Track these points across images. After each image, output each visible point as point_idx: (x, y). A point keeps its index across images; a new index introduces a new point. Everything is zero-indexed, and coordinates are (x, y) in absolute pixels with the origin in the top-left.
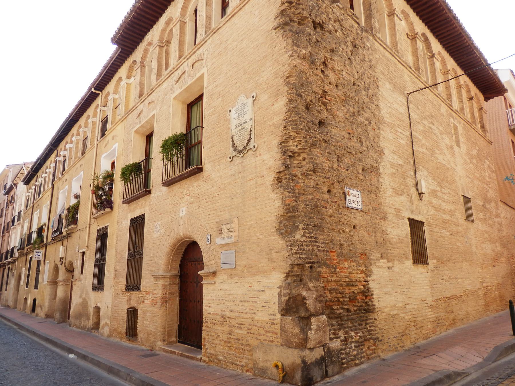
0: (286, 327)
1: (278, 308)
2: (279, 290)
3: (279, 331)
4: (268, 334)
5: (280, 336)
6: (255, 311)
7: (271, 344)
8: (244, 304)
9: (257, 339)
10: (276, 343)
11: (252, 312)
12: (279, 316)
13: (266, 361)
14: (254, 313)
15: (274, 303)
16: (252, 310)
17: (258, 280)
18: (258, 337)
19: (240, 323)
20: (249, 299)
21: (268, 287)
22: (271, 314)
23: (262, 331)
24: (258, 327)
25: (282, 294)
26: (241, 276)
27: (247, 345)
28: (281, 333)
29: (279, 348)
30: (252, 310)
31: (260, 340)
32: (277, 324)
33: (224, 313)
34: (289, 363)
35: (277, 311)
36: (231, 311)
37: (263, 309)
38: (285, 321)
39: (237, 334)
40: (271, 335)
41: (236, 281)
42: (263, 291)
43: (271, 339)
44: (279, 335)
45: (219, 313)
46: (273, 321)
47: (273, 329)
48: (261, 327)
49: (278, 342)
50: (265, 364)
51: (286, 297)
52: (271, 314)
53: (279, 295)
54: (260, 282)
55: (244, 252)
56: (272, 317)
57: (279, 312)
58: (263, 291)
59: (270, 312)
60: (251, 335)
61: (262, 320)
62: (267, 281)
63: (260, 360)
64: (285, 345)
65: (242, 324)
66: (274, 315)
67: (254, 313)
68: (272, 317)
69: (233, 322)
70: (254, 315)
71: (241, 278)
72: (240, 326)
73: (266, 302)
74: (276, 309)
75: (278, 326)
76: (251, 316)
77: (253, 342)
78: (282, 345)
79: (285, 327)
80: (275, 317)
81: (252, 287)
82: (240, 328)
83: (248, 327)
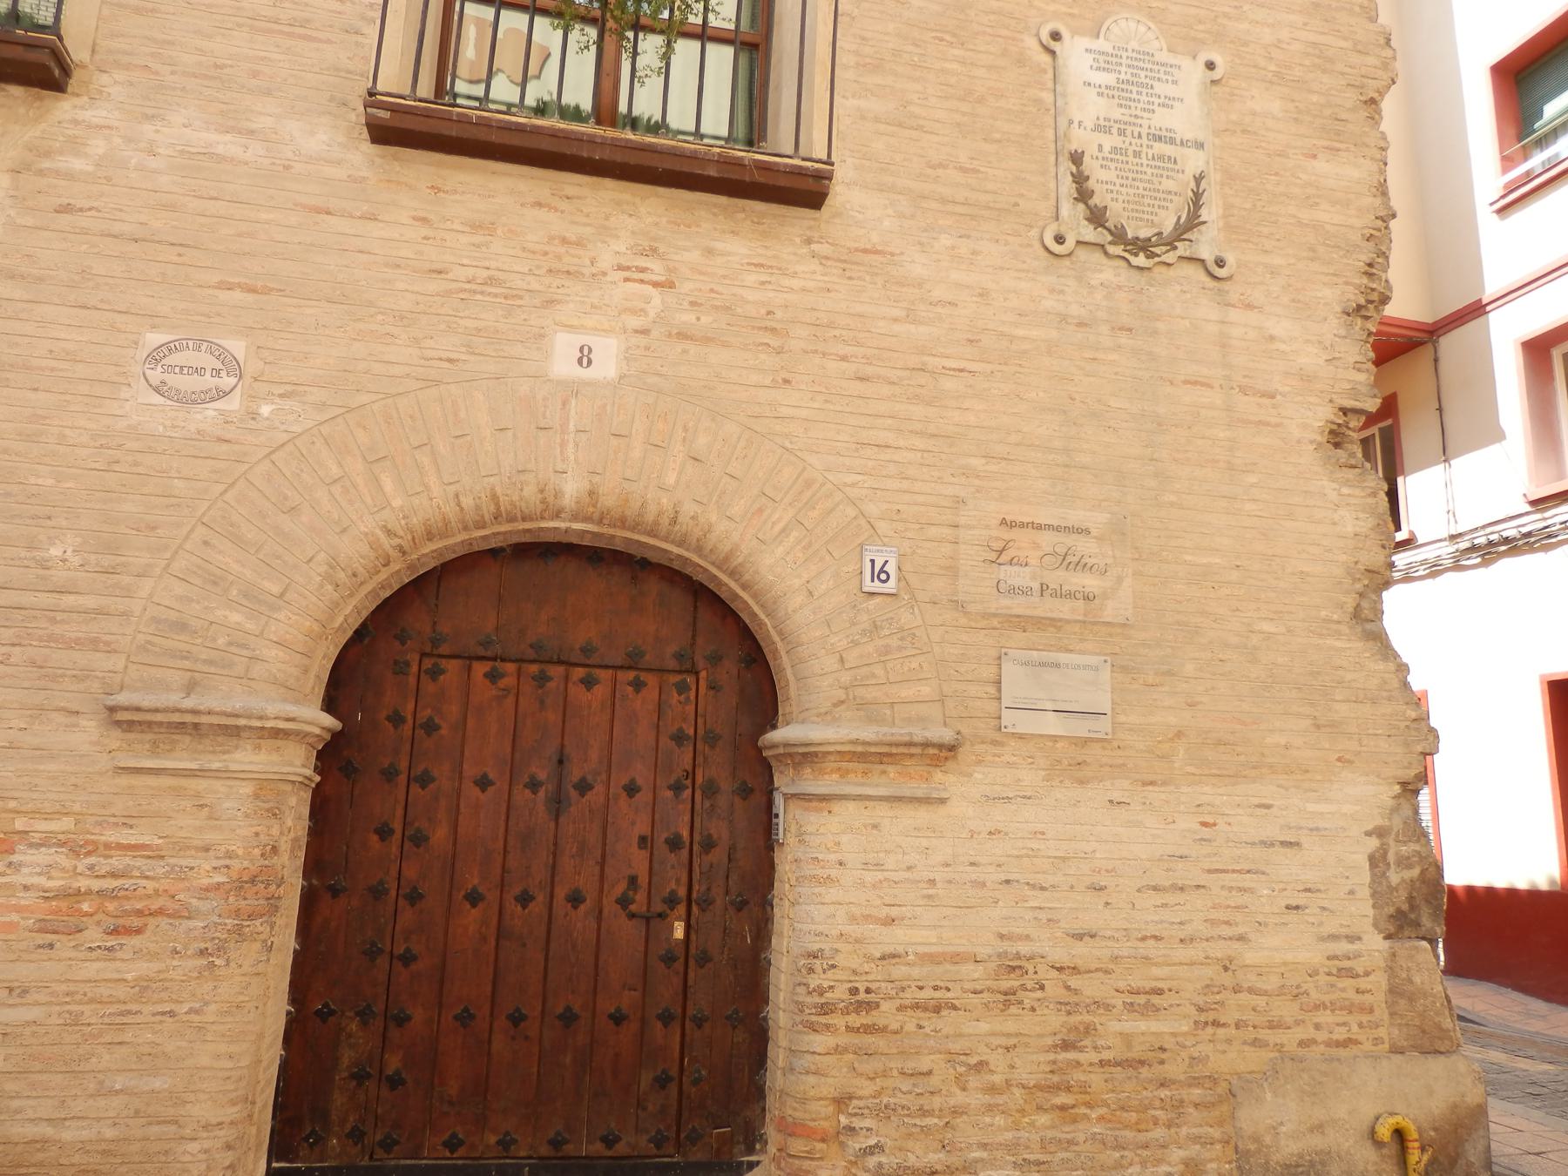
0: (1417, 980)
1: (1371, 912)
2: (1373, 843)
3: (1378, 999)
4: (1325, 1017)
5: (1386, 1017)
6: (1241, 930)
7: (1343, 1053)
8: (1170, 898)
9: (1255, 1043)
10: (1367, 1046)
11: (1227, 931)
12: (1375, 944)
13: (1319, 1128)
14: (1241, 938)
15: (1351, 892)
16: (1227, 923)
17: (1256, 801)
18: (1264, 1034)
19: (1149, 985)
20: (1203, 879)
21: (1317, 829)
22: (1334, 937)
23: (1286, 1010)
24: (1265, 993)
25: (1391, 857)
26: (1151, 778)
27: (1195, 1082)
28: (1390, 1005)
29: (1385, 1063)
30: (1227, 923)
31: (1279, 1047)
32: (1367, 974)
33: (1024, 948)
34: (1436, 1112)
35: (1371, 920)
36: (1079, 937)
37: (1293, 917)
38: (1411, 957)
39: (1127, 1038)
40: (1341, 1020)
41: (1117, 796)
42: (1288, 844)
43: (1340, 1034)
44: (1381, 1013)
45: (982, 952)
46: (1346, 964)
47: (1351, 994)
48: (1281, 991)
49: (1377, 1041)
50: (1317, 1142)
51: (1410, 867)
52: (1334, 937)
53: (1377, 861)
54: (1268, 807)
55: (1170, 673)
56: (1344, 947)
57: (1375, 925)
58: (1288, 844)
59: (1331, 926)
60: (1221, 1032)
61: (1285, 964)
62: (1311, 807)
63: (1284, 1129)
64: (1415, 1047)
65: (1159, 992)
66: (1353, 938)
67: (1241, 938)
68: (1344, 947)
69: (1091, 988)
70: (1237, 945)
71: (1152, 783)
72: (1147, 1000)
73: (1308, 890)
74: (1361, 913)
75: (1379, 981)
76: (1218, 950)
77: (1231, 1059)
78: (1396, 1050)
79: (1410, 981)
80: (1356, 946)
81: (1222, 826)
82: (1149, 1010)
83: (1200, 1000)
